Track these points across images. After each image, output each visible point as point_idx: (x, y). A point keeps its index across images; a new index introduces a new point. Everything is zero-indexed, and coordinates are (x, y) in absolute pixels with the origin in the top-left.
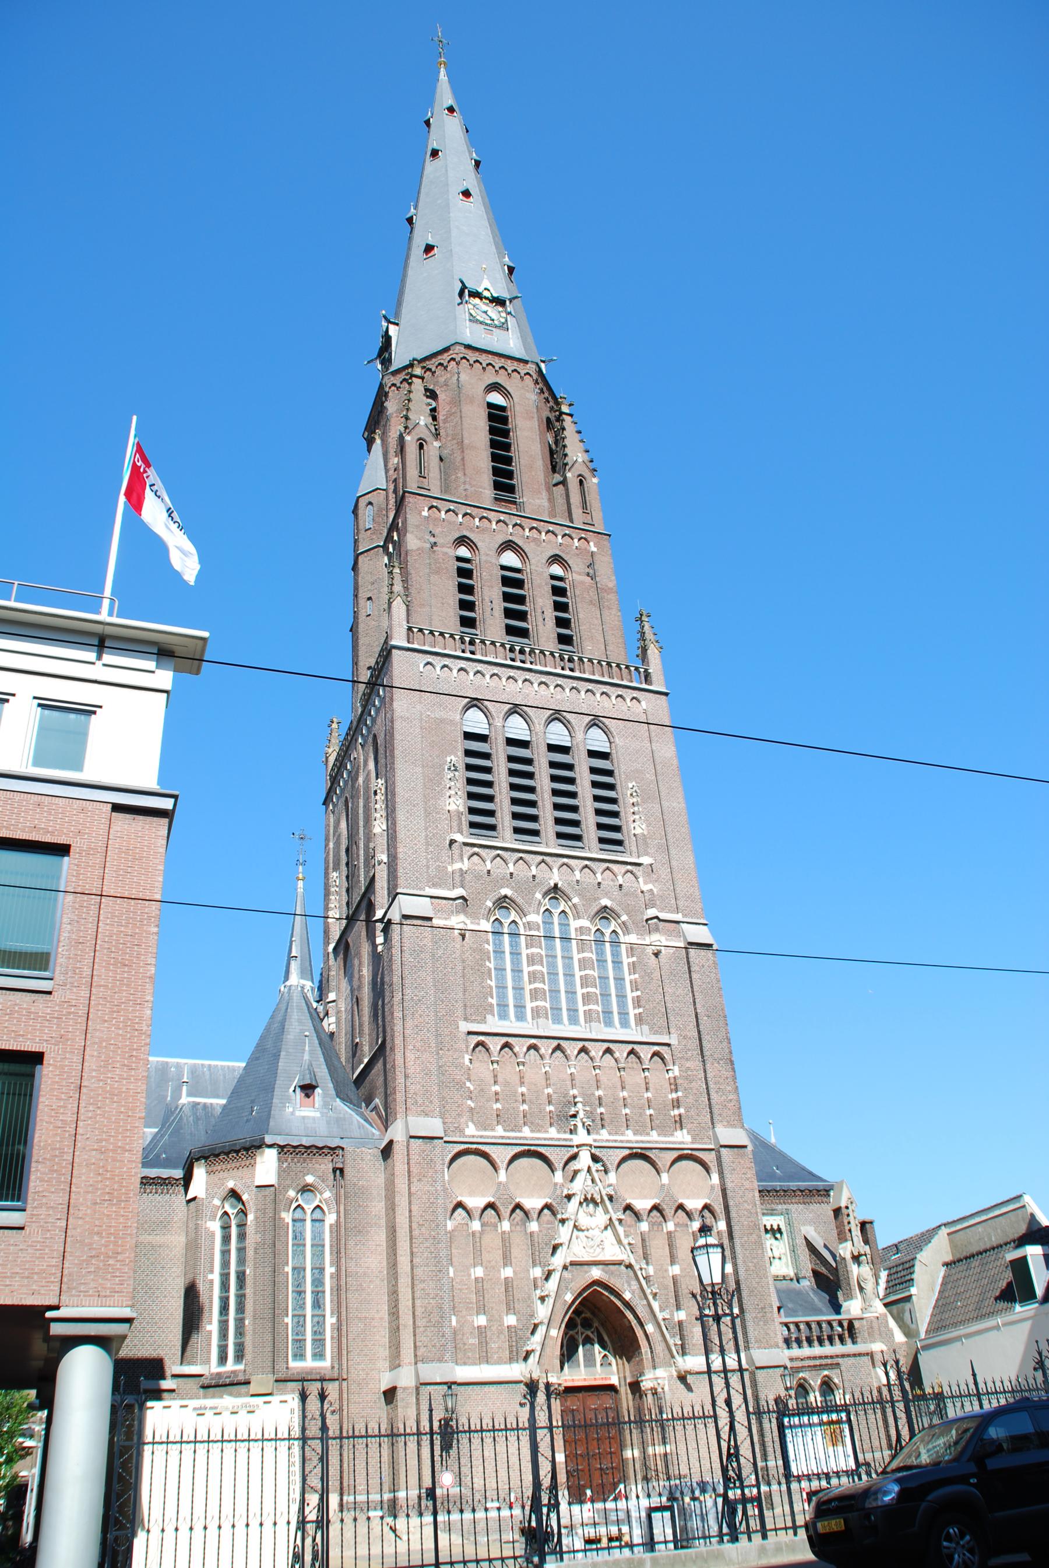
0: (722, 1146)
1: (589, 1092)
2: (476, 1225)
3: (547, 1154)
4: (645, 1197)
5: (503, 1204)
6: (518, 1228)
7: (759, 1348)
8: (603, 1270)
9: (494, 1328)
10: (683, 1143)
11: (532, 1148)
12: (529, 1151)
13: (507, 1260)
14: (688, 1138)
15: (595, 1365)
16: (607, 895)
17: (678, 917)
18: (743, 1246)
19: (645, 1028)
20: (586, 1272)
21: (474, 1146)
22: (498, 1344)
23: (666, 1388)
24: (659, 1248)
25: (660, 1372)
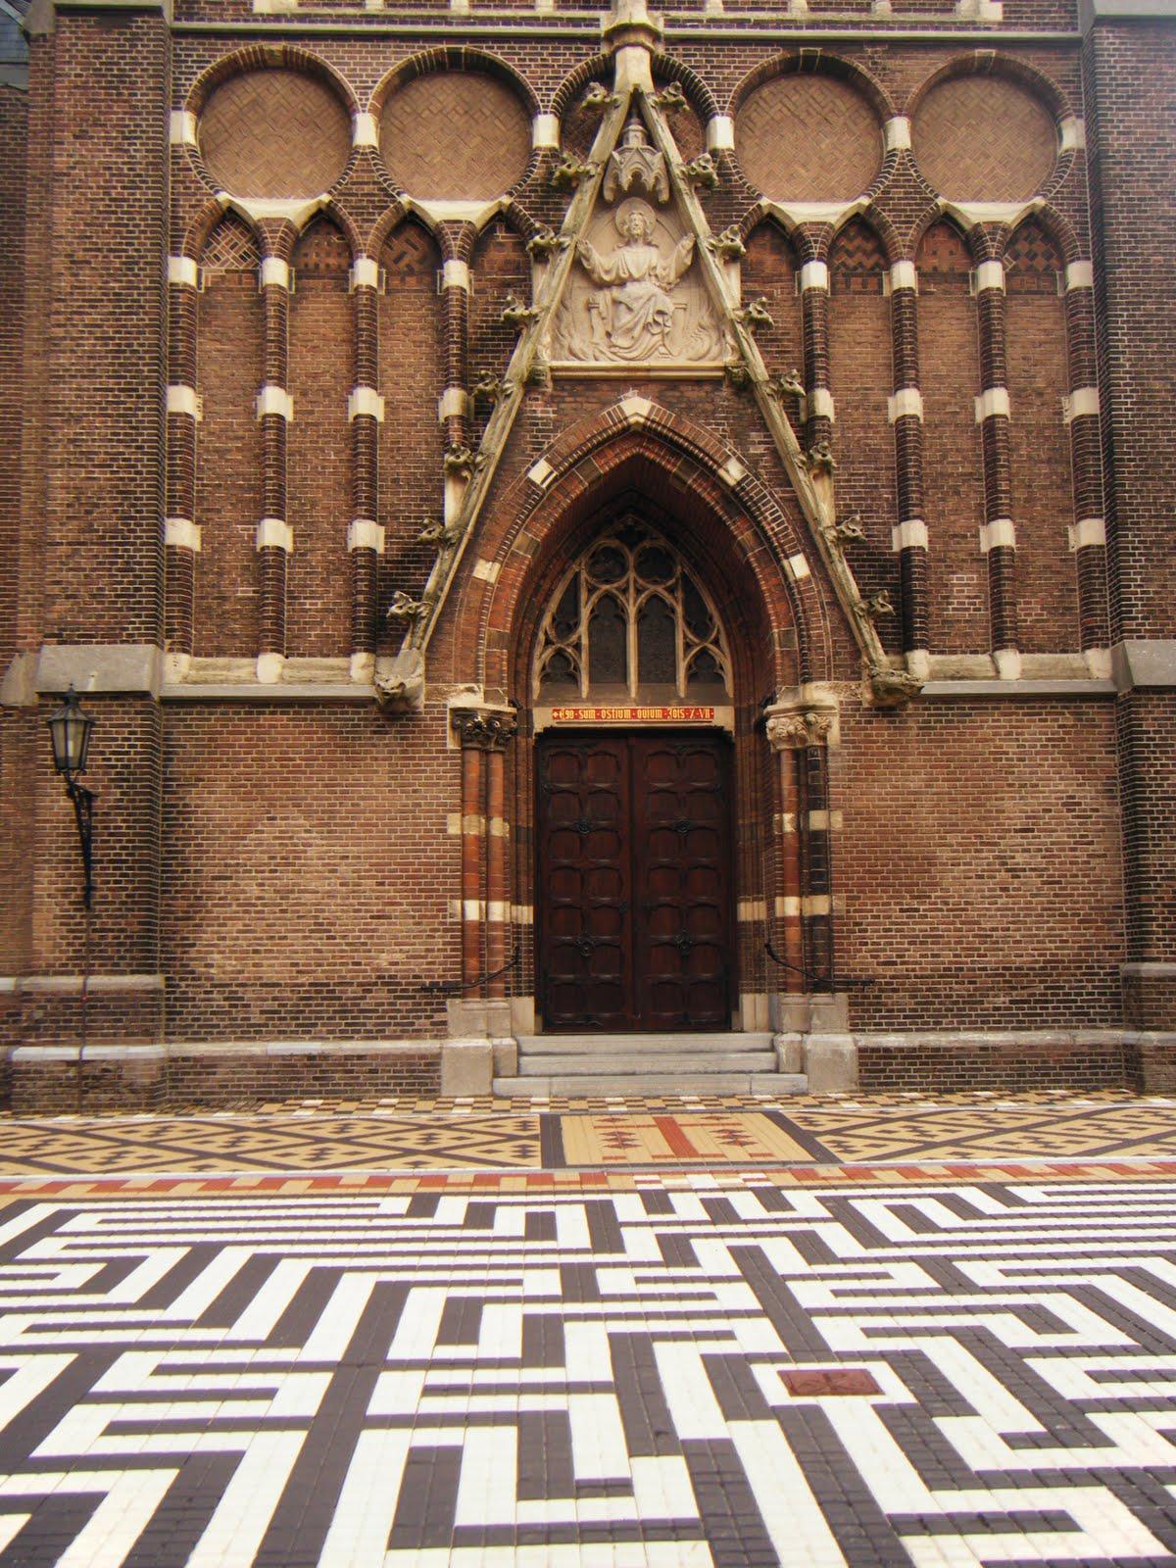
2: (276, 272)
3: (513, 65)
4: (830, 196)
5: (358, 211)
6: (411, 281)
7: (1154, 634)
8: (659, 398)
9: (314, 559)
10: (973, 25)
11: (464, 47)
12: (454, 55)
13: (363, 368)
15: (673, 679)
18: (1136, 328)
20: (605, 404)
21: (277, 46)
22: (319, 603)
23: (834, 735)
24: (858, 342)
25: (822, 693)
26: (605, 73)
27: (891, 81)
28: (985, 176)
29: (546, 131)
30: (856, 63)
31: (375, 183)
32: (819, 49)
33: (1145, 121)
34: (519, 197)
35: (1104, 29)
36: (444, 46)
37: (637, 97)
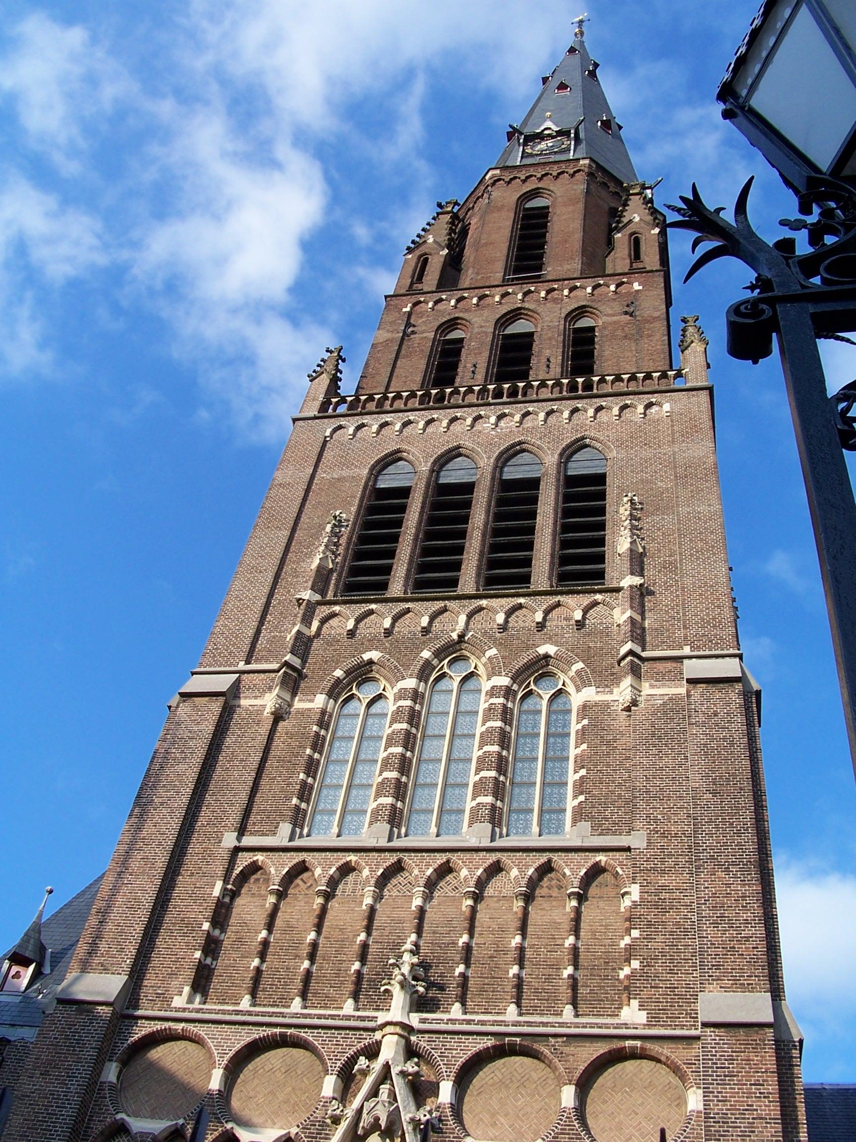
0: (705, 1025)
1: (446, 940)
10: (626, 1026)
11: (289, 1031)
12: (283, 1035)
14: (642, 1017)
16: (550, 640)
17: (687, 651)
19: (586, 826)
21: (180, 1026)
26: (372, 1052)
27: (566, 1061)
28: (634, 1128)
29: (329, 1085)
30: (542, 1049)
31: (214, 1114)
32: (518, 1039)
33: (738, 1093)
34: (303, 1128)
35: (708, 1030)
36: (278, 1030)
37: (387, 1067)
